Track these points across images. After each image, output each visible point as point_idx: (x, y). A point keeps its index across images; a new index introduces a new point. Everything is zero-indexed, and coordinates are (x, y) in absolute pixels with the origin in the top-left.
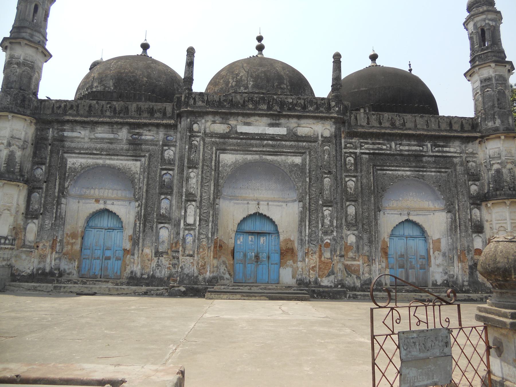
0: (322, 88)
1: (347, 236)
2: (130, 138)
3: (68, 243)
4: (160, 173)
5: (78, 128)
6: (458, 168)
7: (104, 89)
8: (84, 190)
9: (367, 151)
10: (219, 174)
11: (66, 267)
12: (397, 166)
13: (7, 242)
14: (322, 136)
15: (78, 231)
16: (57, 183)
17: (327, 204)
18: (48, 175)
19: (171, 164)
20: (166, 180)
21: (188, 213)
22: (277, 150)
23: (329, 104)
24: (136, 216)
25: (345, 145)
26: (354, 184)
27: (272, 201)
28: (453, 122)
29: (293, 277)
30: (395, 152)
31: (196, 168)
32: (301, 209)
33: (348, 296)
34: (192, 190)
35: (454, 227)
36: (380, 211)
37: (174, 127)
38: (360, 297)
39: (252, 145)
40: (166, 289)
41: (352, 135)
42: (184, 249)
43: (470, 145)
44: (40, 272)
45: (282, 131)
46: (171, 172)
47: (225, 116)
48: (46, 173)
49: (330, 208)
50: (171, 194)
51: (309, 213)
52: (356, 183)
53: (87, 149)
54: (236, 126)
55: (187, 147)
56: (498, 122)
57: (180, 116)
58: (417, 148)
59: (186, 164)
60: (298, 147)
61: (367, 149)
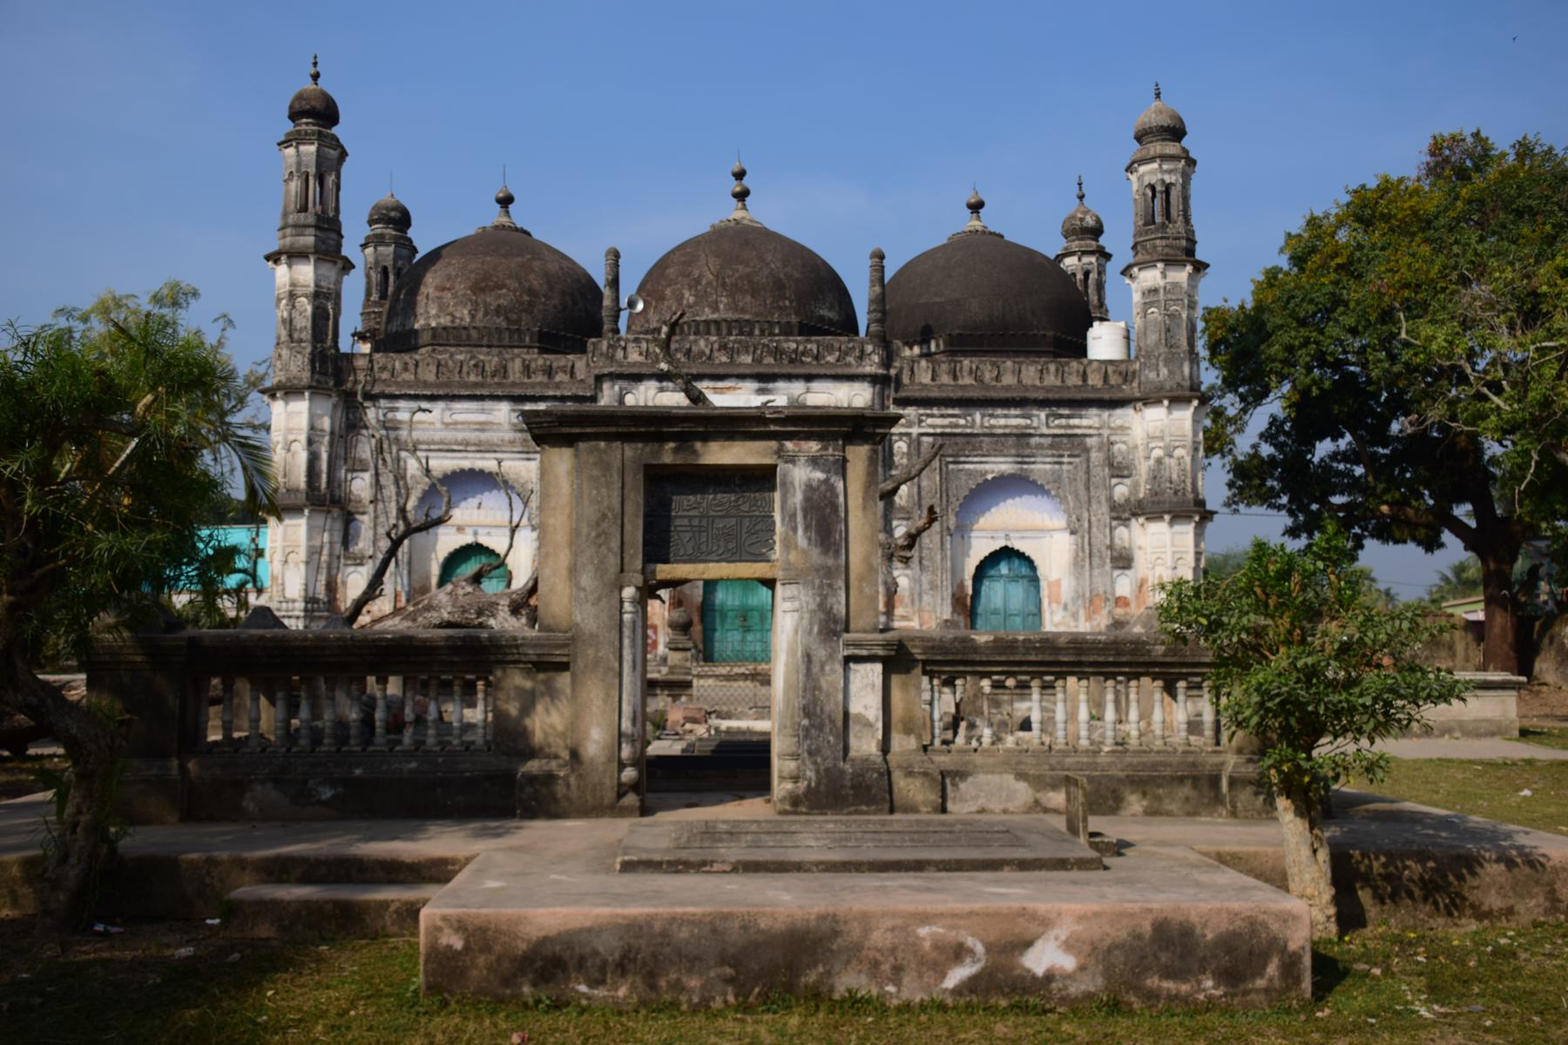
6: (1094, 455)
9: (931, 431)
23: (862, 351)
28: (1089, 370)
35: (1085, 557)
43: (1118, 412)
53: (442, 442)
56: (1164, 371)
57: (599, 379)
58: (1022, 422)
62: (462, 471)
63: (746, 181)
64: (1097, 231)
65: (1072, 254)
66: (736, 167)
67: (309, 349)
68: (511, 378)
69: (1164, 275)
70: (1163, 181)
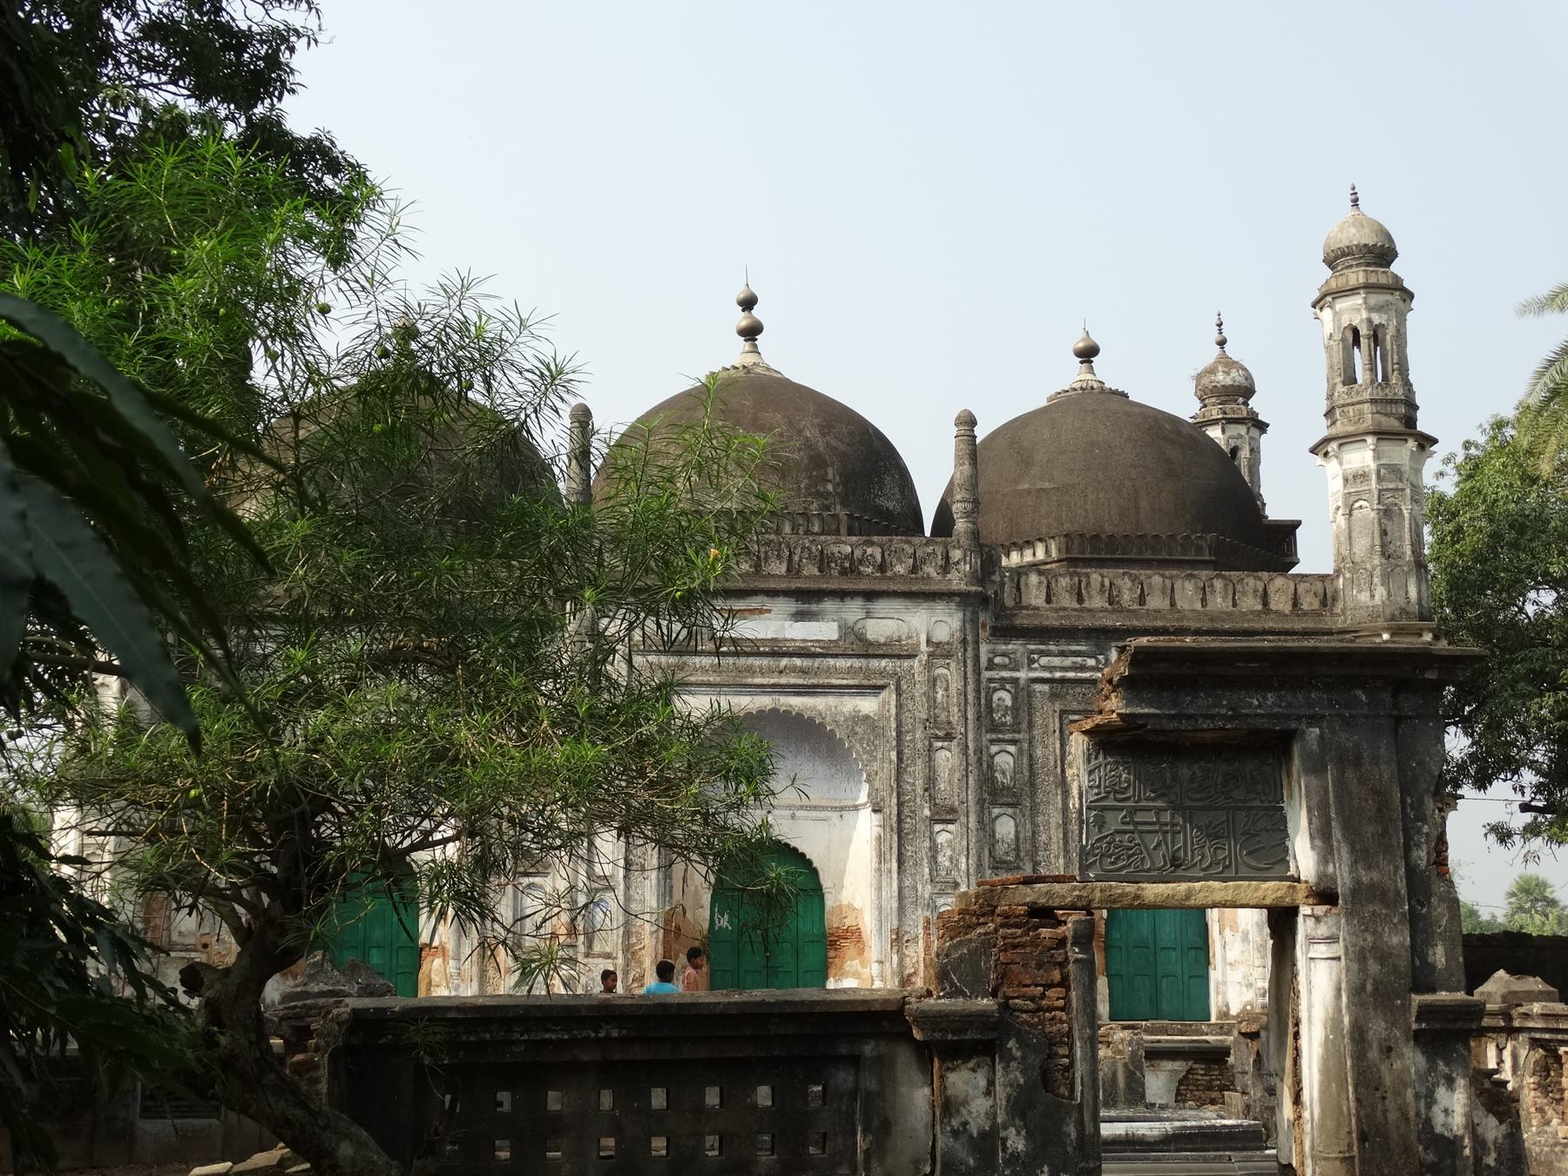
0: (932, 474)
9: (1047, 675)
14: (928, 641)
17: (944, 815)
22: (815, 681)
23: (947, 558)
25: (990, 661)
26: (1011, 760)
28: (1271, 589)
32: (880, 830)
39: (750, 670)
41: (1006, 631)
45: (823, 630)
49: (951, 827)
51: (900, 838)
56: (1380, 592)
60: (868, 673)
61: (1045, 668)
63: (757, 312)
64: (1248, 391)
65: (1214, 422)
66: (740, 292)
69: (1377, 455)
70: (1370, 321)
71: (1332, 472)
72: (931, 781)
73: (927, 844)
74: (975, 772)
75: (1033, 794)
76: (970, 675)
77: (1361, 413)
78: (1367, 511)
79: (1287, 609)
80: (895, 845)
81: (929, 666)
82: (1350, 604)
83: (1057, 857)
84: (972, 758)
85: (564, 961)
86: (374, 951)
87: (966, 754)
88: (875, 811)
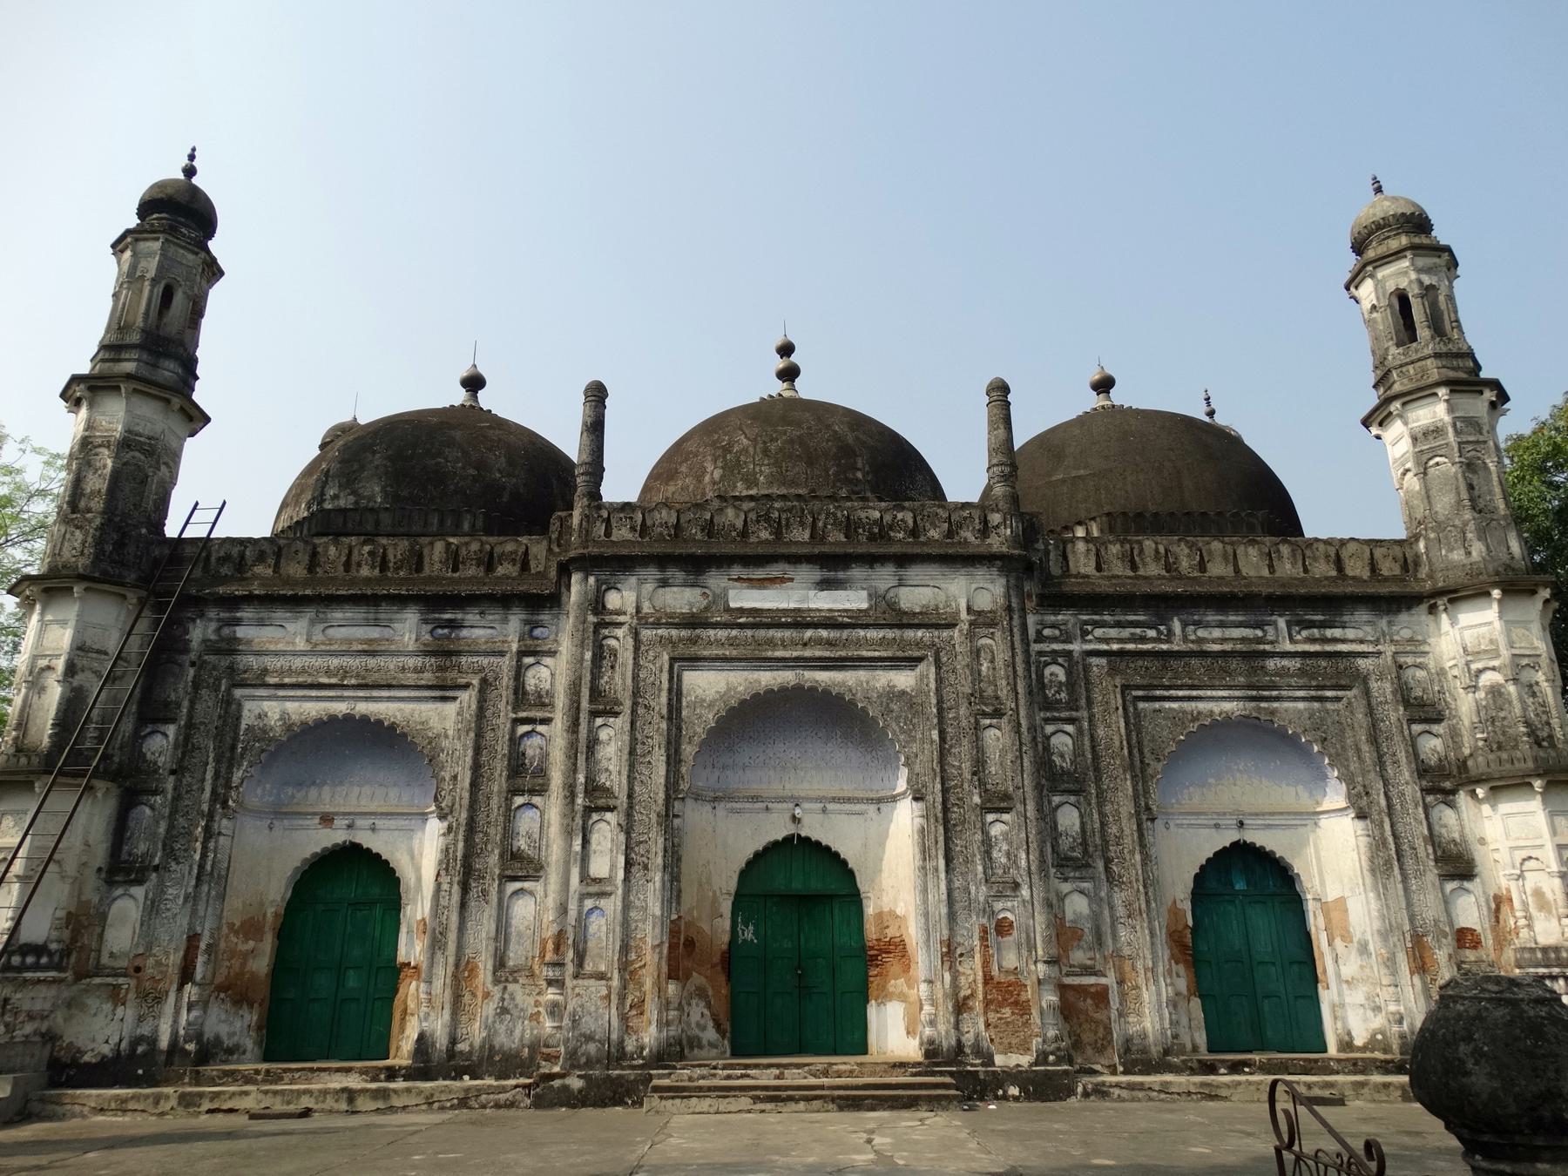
0: (963, 474)
1: (1062, 898)
2: (428, 637)
3: (233, 954)
4: (513, 731)
5: (280, 614)
7: (356, 503)
8: (290, 791)
9: (1105, 647)
10: (679, 729)
11: (223, 1030)
12: (1192, 687)
13: (44, 960)
14: (969, 610)
15: (265, 915)
16: (209, 775)
17: (997, 802)
18: (184, 754)
19: (544, 705)
20: (530, 752)
21: (594, 845)
22: (843, 654)
23: (985, 522)
24: (440, 863)
25: (1039, 632)
26: (1069, 741)
27: (834, 800)
28: (1345, 554)
29: (910, 1032)
30: (1183, 647)
31: (616, 714)
33: (1080, 1089)
34: (602, 778)
36: (1153, 820)
37: (553, 601)
38: (1117, 1091)
39: (771, 643)
40: (524, 1086)
41: (1054, 599)
42: (580, 958)
43: (1403, 617)
44: (140, 1049)
45: (853, 600)
46: (540, 728)
47: (696, 565)
48: (176, 745)
49: (1006, 817)
50: (541, 790)
51: (947, 835)
52: (1077, 738)
53: (303, 671)
54: (726, 590)
55: (588, 655)
56: (1478, 550)
57: (565, 570)
59: (585, 704)
62: (333, 719)
63: (794, 358)
66: (779, 341)
67: (98, 521)
68: (427, 571)
69: (1451, 410)
70: (1420, 282)
71: (1397, 440)
72: (979, 764)
73: (978, 837)
74: (1031, 753)
75: (1098, 780)
76: (1017, 644)
77: (1424, 371)
78: (1446, 467)
79: (1366, 574)
80: (941, 839)
81: (971, 636)
82: (1438, 565)
83: (1132, 852)
84: (1026, 737)
85: (550, 983)
86: (351, 972)
87: (1018, 732)
88: (916, 799)
